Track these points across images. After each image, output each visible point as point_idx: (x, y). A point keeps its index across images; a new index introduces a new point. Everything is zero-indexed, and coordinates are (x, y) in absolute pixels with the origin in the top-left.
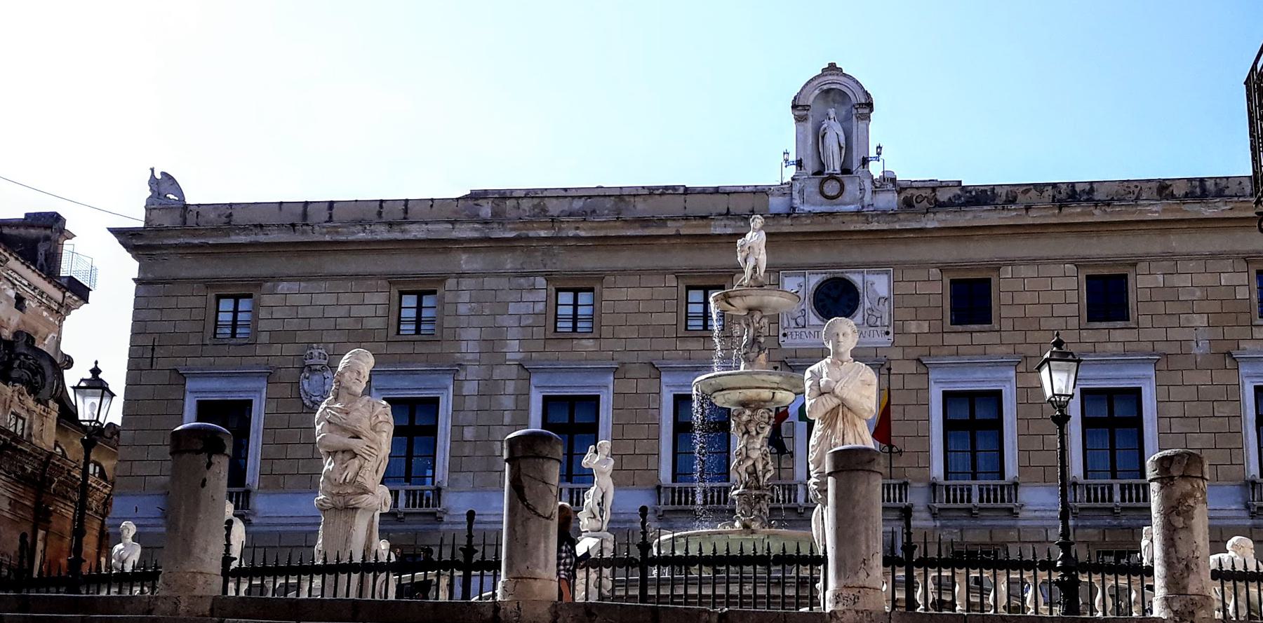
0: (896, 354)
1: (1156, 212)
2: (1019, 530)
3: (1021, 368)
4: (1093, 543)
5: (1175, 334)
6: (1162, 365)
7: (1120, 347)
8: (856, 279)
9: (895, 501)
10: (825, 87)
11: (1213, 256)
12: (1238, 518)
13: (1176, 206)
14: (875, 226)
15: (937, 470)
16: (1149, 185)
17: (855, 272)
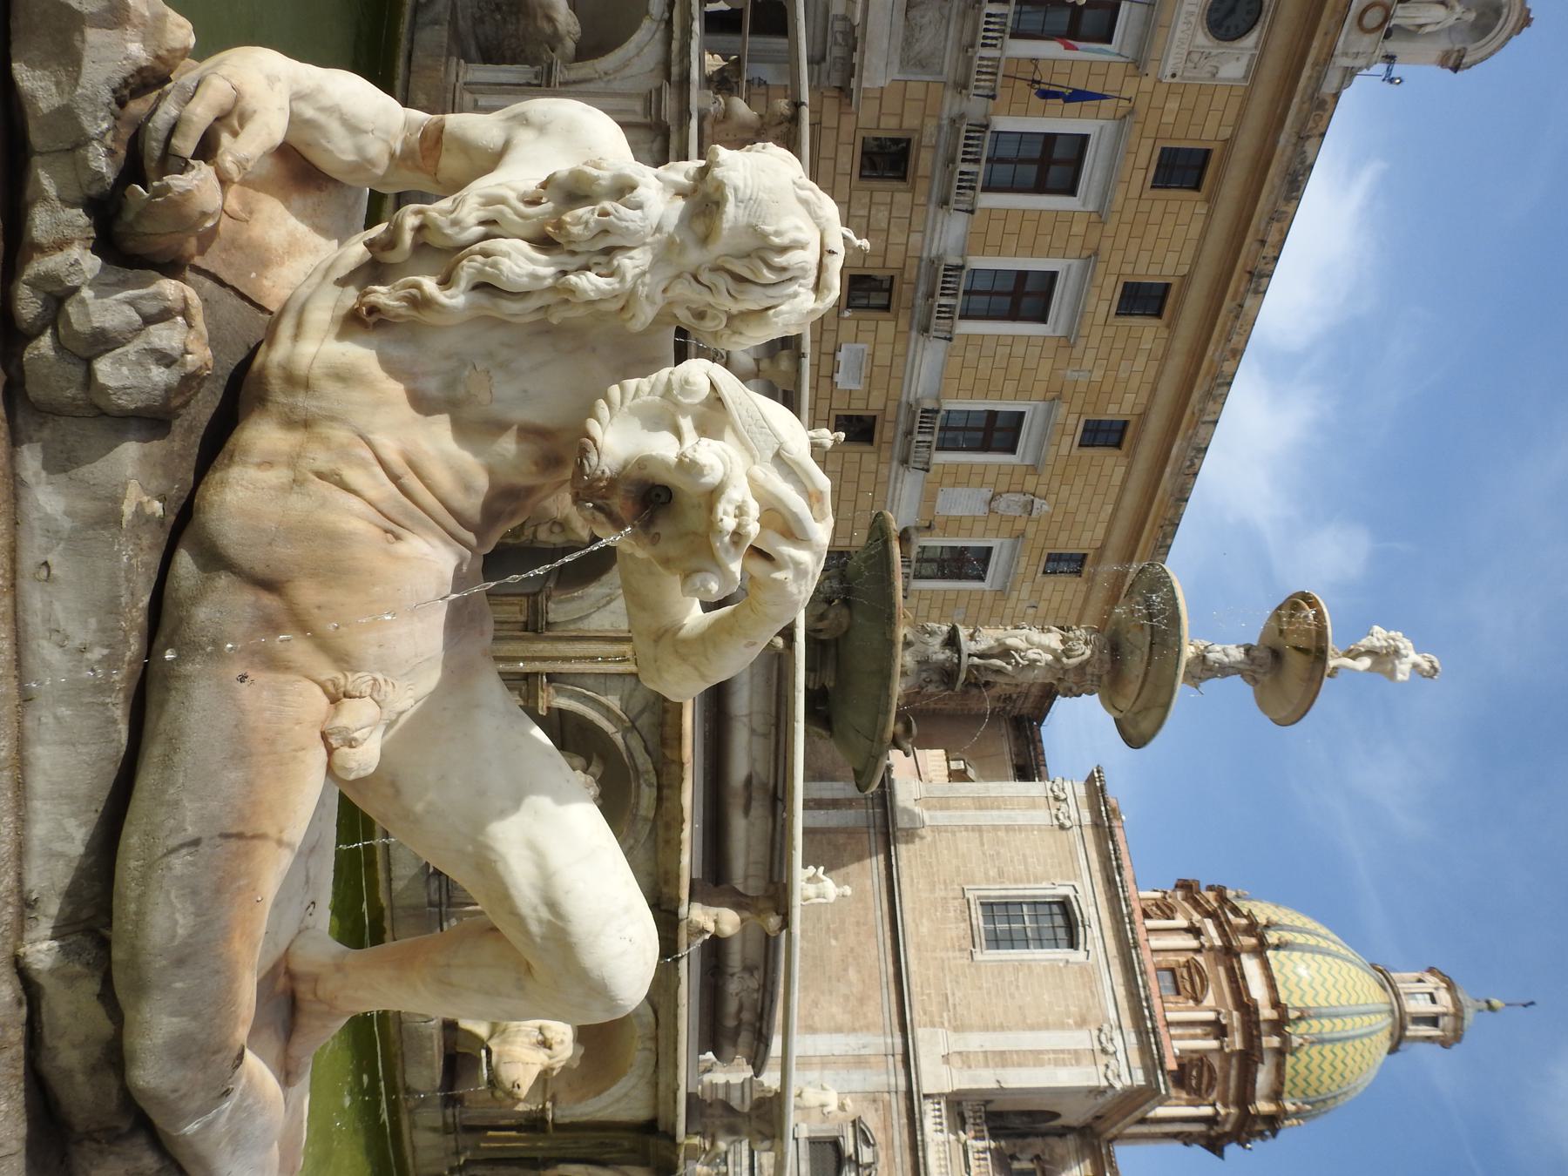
0: (1147, 84)
1: (1213, 354)
2: (924, 205)
3: (1094, 217)
4: (902, 275)
5: (1091, 354)
6: (1063, 340)
7: (1090, 308)
8: (1250, 40)
9: (977, 80)
10: (1505, 11)
11: (1154, 392)
12: (909, 392)
13: (1213, 371)
14: (1306, 72)
15: (1004, 123)
16: (1243, 343)
17: (1259, 37)
